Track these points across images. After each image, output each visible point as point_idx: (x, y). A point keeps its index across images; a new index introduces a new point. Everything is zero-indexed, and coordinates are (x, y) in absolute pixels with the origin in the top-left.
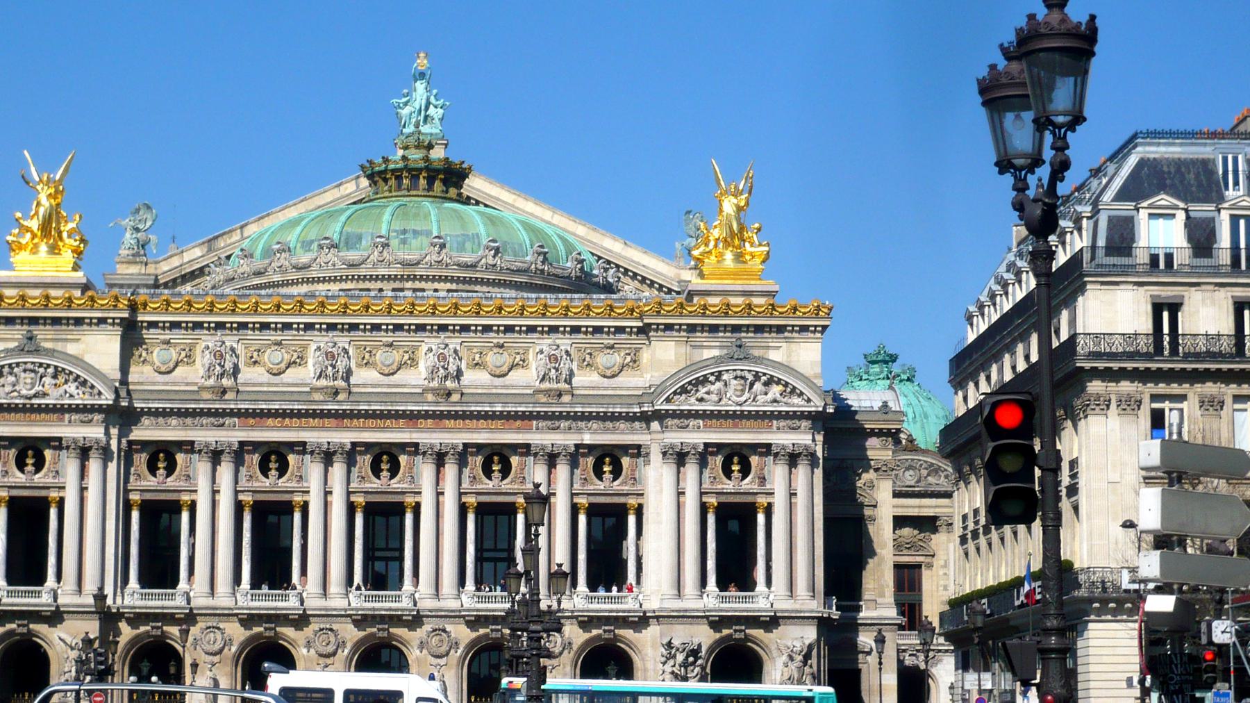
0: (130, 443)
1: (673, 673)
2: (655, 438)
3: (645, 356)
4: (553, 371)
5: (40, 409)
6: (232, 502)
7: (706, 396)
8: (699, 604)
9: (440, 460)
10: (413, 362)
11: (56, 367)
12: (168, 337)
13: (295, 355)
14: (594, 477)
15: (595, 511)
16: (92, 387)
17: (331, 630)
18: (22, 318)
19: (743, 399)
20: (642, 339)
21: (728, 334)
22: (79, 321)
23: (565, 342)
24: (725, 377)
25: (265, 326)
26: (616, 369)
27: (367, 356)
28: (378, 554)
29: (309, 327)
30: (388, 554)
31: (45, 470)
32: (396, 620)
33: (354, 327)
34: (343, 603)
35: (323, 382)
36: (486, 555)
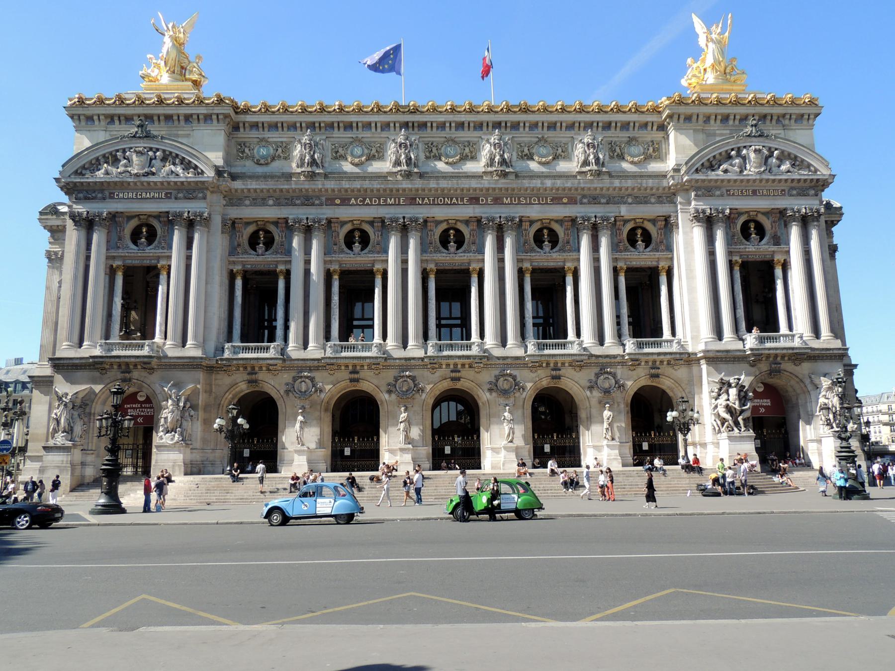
4: (592, 156)
5: (150, 187)
11: (164, 151)
14: (628, 245)
15: (630, 271)
16: (196, 167)
19: (762, 169)
20: (661, 134)
21: (737, 122)
22: (188, 118)
24: (744, 152)
25: (349, 126)
27: (434, 149)
28: (443, 322)
29: (386, 126)
31: (156, 242)
33: (423, 125)
34: (420, 353)
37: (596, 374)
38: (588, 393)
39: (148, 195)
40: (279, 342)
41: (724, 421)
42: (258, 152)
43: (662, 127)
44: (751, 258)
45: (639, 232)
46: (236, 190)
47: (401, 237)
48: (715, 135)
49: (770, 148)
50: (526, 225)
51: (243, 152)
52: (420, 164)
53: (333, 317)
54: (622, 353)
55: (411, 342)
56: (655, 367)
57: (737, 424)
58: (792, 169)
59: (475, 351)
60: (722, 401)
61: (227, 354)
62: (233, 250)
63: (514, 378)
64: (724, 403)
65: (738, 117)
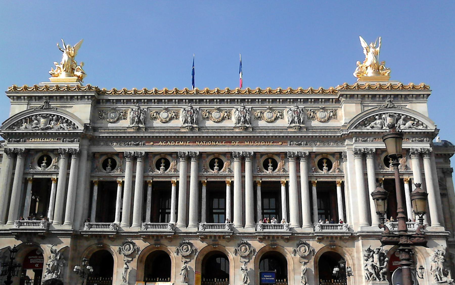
0: (94, 154)
1: (373, 264)
3: (341, 112)
4: (296, 118)
6: (142, 181)
7: (374, 125)
9: (242, 159)
10: (229, 117)
11: (58, 116)
12: (115, 107)
13: (174, 114)
17: (189, 243)
18: (46, 96)
21: (381, 99)
22: (72, 97)
23: (301, 106)
24: (384, 116)
25: (160, 101)
26: (326, 118)
32: (222, 237)
34: (195, 230)
35: (186, 125)
36: (265, 211)
37: (297, 244)
38: (293, 255)
39: (48, 140)
41: (371, 274)
42: (110, 115)
45: (325, 161)
46: (96, 137)
47: (187, 163)
48: (368, 106)
49: (399, 114)
51: (102, 115)
52: (199, 122)
53: (147, 208)
54: (312, 231)
55: (191, 223)
57: (378, 275)
58: (412, 126)
60: (370, 262)
61: (85, 228)
62: (93, 169)
64: (371, 263)
65: (381, 96)
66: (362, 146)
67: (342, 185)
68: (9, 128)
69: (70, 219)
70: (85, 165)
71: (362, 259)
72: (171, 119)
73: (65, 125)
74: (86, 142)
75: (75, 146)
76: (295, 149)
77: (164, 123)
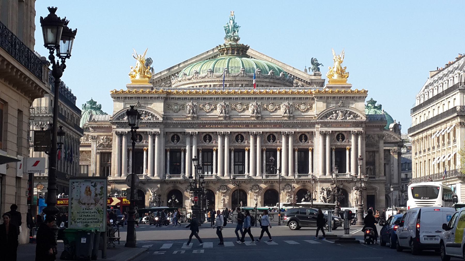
2: (317, 129)
3: (314, 106)
8: (331, 177)
9: (255, 136)
20: (313, 101)
24: (337, 112)
25: (205, 99)
28: (236, 163)
30: (239, 163)
32: (244, 181)
40: (182, 174)
43: (313, 99)
44: (339, 147)
45: (303, 136)
48: (330, 103)
50: (264, 134)
55: (226, 174)
56: (304, 183)
59: (246, 177)
61: (167, 178)
62: (166, 142)
63: (259, 186)
66: (324, 129)
67: (312, 151)
68: (118, 119)
69: (158, 173)
70: (163, 140)
71: (319, 193)
72: (212, 110)
73: (150, 117)
74: (162, 126)
75: (158, 130)
76: (287, 130)
77: (208, 113)
